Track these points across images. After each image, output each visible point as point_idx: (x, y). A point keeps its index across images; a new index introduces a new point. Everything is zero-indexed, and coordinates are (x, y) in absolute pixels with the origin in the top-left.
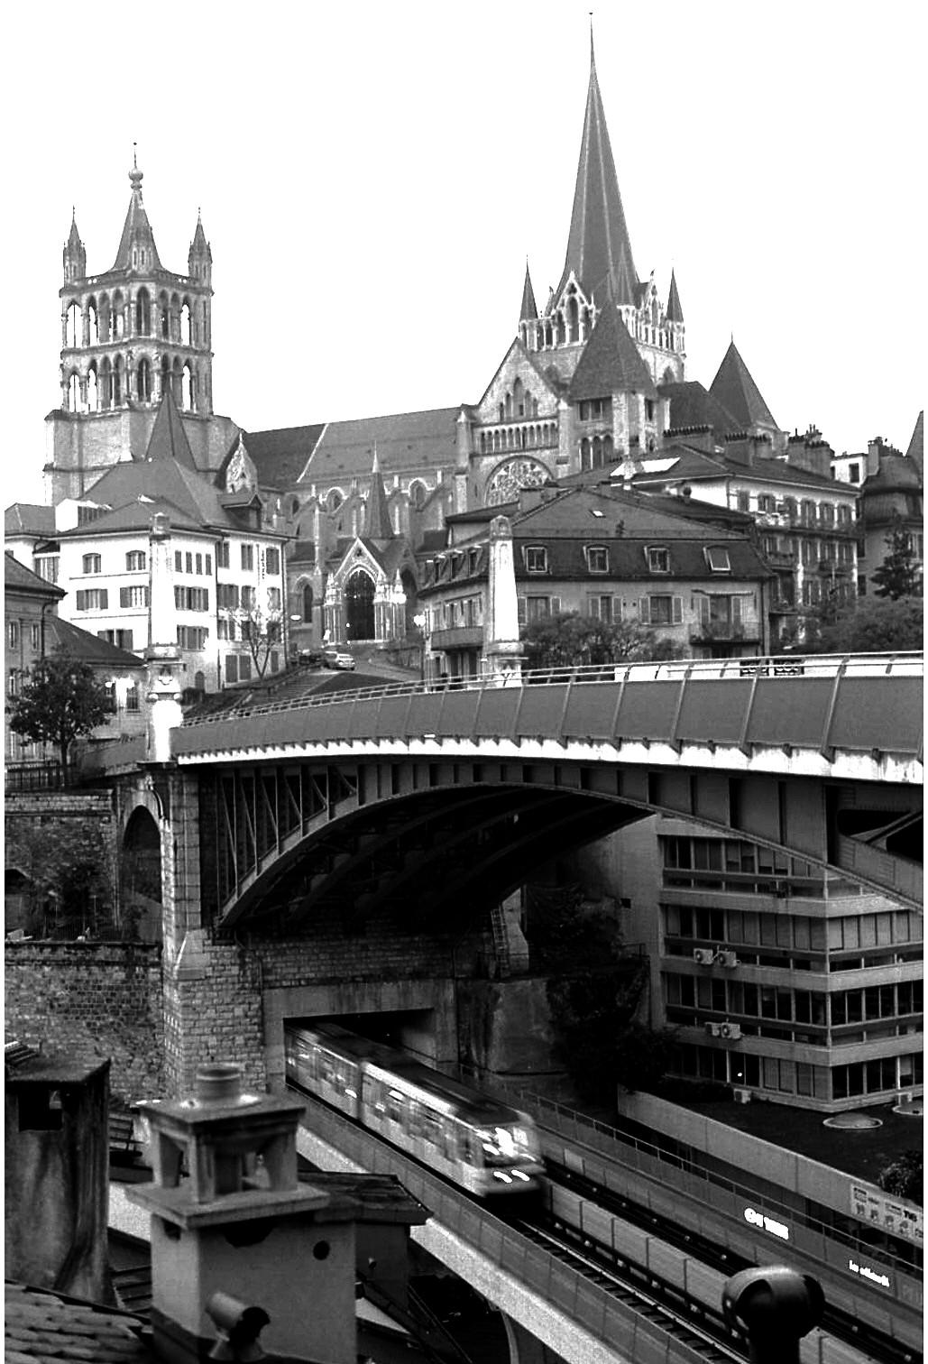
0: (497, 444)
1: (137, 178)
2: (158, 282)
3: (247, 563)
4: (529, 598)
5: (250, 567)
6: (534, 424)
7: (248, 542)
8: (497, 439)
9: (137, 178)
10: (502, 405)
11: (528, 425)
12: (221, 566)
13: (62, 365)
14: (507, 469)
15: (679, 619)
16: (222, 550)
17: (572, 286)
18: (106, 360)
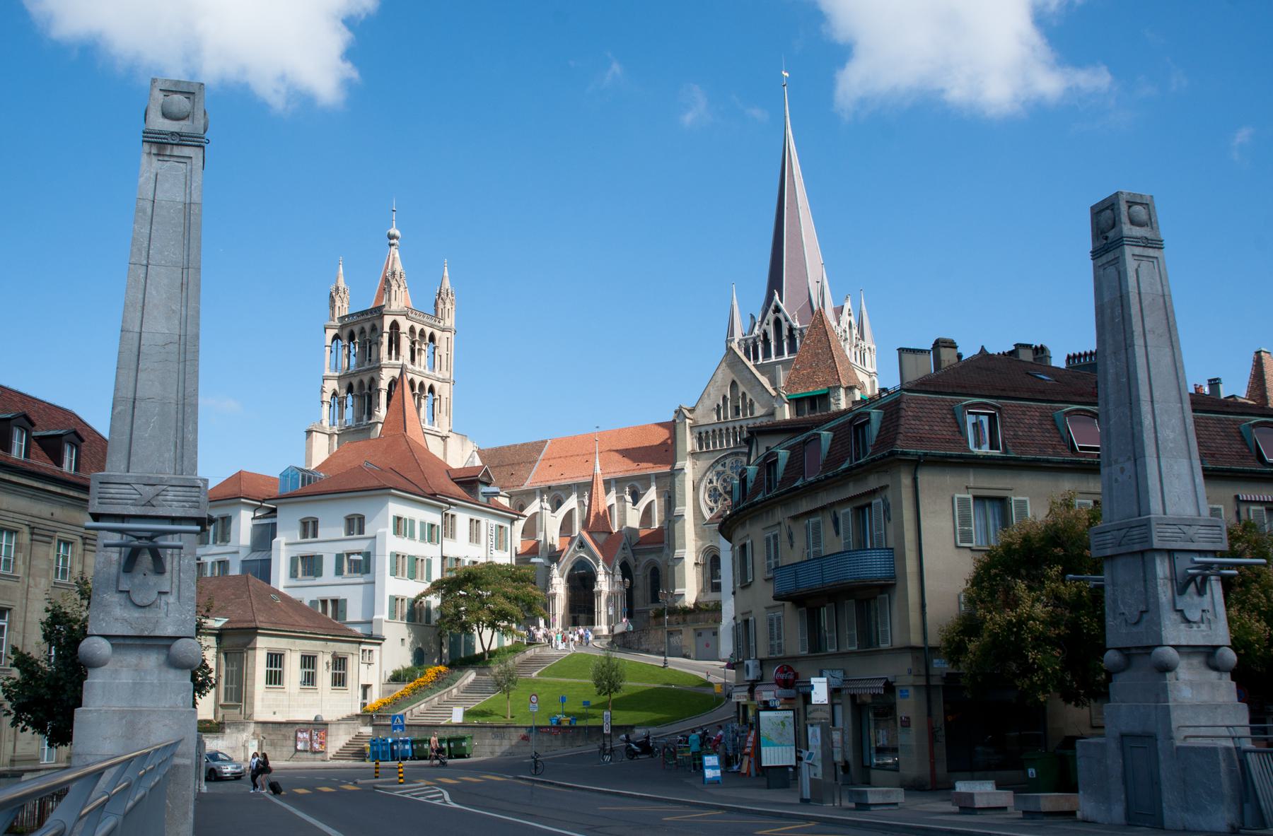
2: (407, 317)
3: (474, 537)
4: (975, 498)
5: (478, 541)
7: (476, 517)
8: (714, 437)
10: (718, 406)
14: (724, 465)
16: (449, 521)
18: (361, 382)
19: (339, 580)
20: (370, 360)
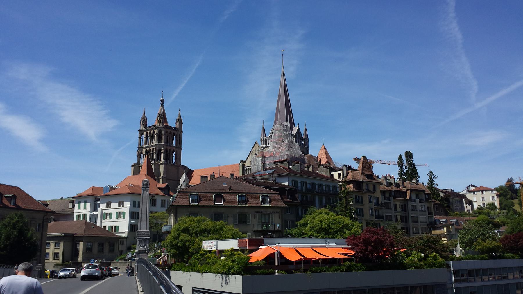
12: (152, 205)
15: (249, 222)
19: (117, 220)
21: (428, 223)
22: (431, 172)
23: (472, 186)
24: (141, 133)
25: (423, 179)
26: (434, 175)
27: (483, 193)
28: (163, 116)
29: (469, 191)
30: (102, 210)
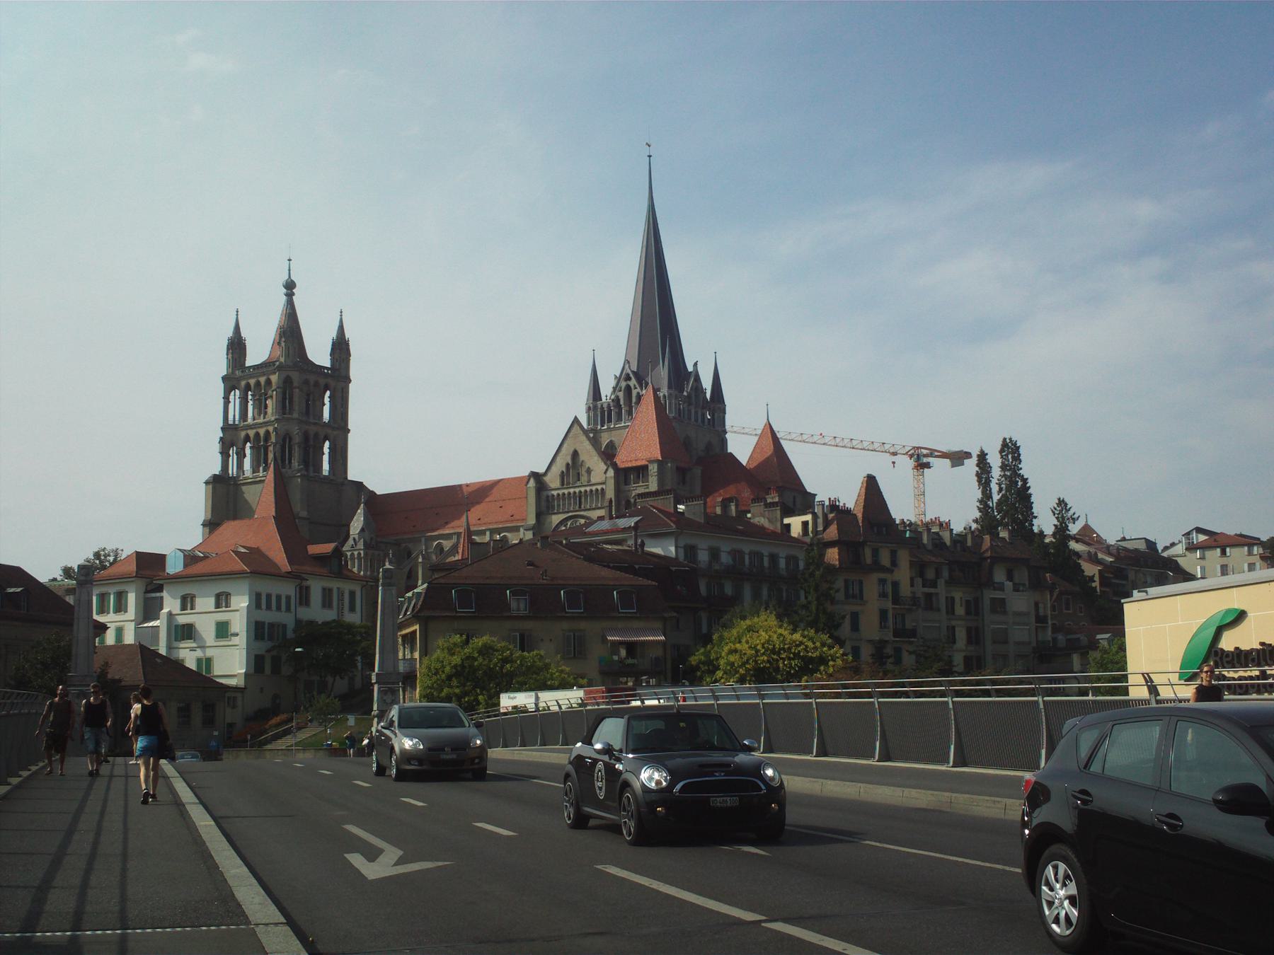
0: (559, 505)
1: (290, 286)
6: (588, 489)
8: (559, 501)
9: (290, 286)
11: (583, 489)
12: (301, 604)
13: (221, 438)
17: (628, 375)
18: (257, 434)
20: (266, 413)
21: (1034, 644)
22: (1061, 502)
23: (1200, 530)
24: (230, 383)
25: (1045, 523)
26: (1071, 512)
27: (1224, 553)
28: (290, 332)
29: (1191, 548)
30: (170, 615)
